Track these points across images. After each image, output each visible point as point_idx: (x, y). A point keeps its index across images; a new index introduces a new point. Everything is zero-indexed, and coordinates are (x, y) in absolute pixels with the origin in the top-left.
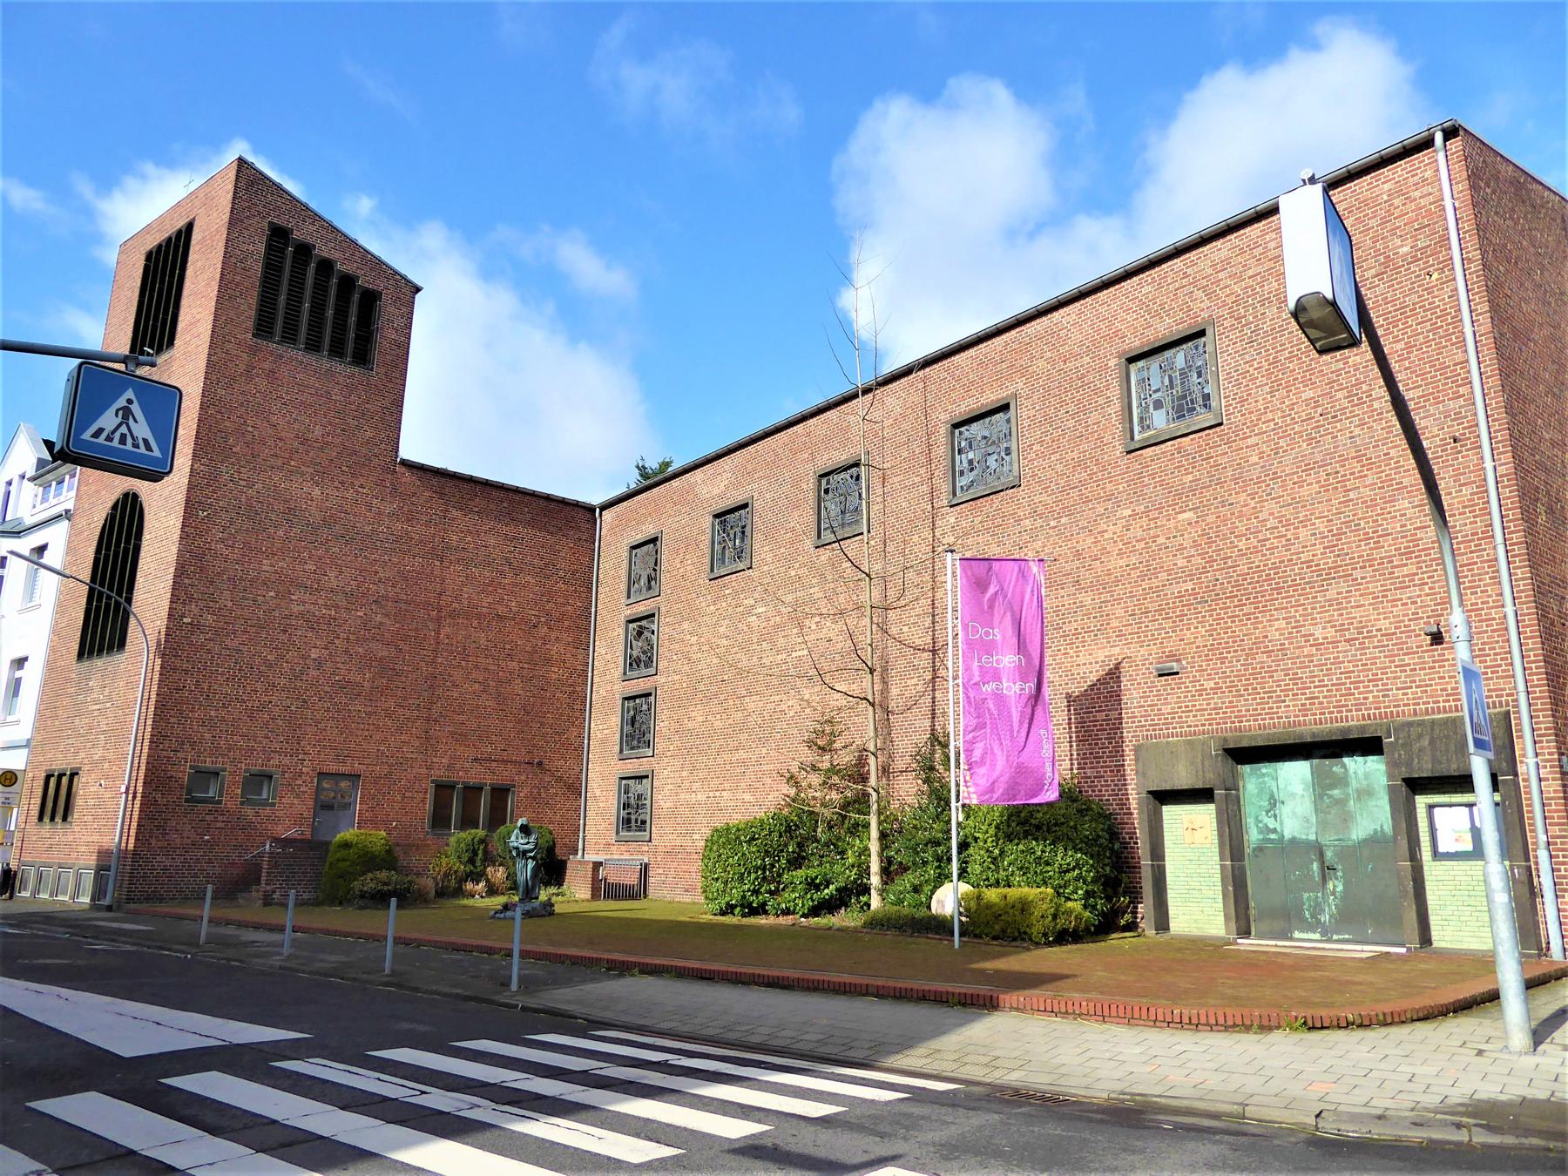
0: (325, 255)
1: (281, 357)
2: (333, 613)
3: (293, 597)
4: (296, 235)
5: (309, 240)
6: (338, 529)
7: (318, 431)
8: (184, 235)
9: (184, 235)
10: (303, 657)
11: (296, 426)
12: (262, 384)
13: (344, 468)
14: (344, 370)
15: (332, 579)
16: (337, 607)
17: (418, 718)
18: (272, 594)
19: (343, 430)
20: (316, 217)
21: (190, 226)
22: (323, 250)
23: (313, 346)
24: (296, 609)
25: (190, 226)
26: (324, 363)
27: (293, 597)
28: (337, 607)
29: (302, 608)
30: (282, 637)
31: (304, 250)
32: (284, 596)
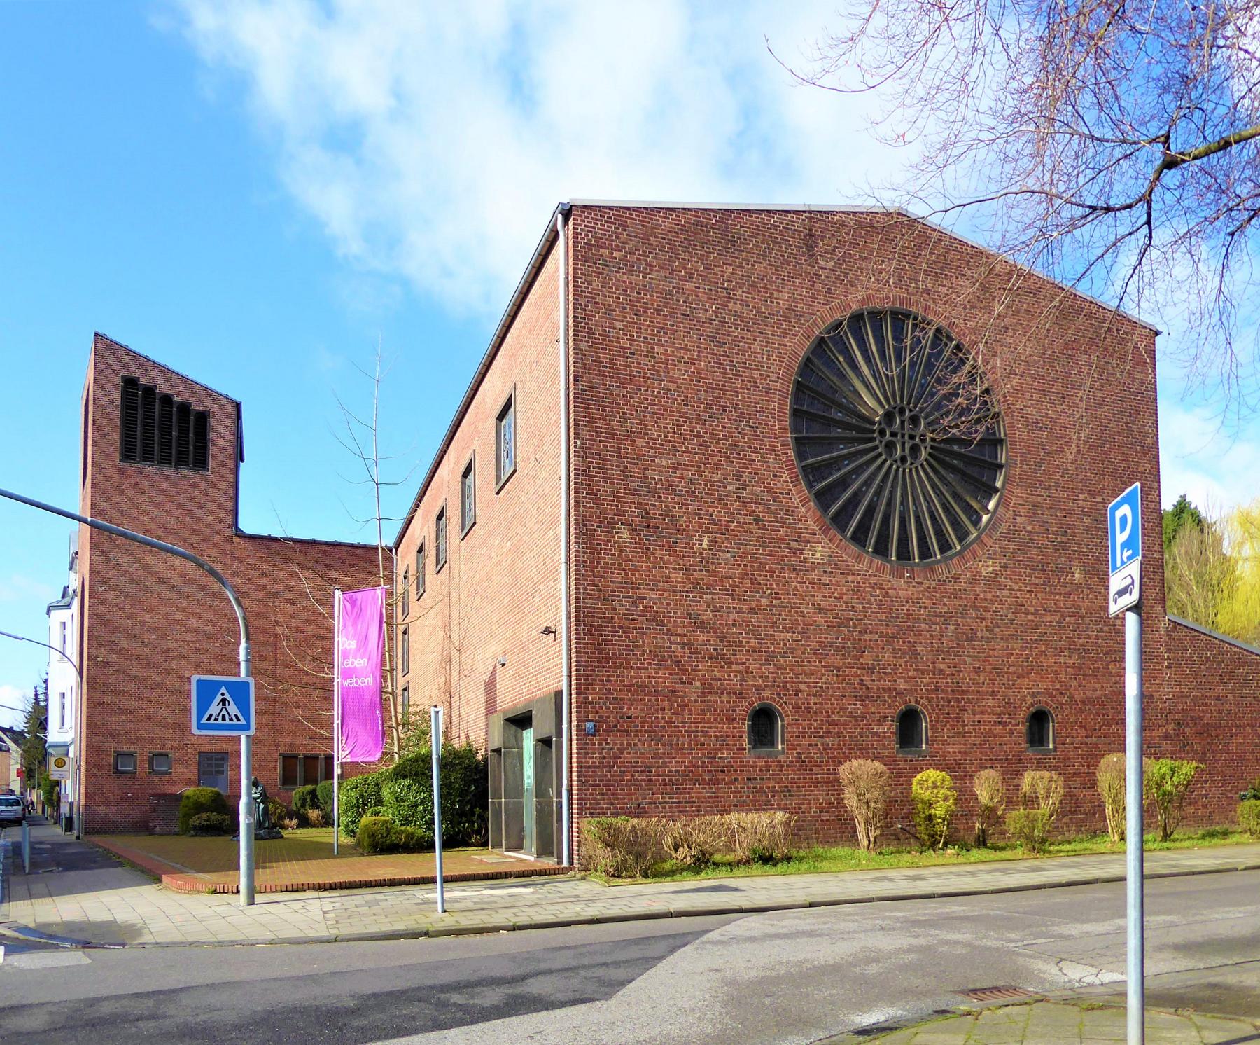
0: (164, 391)
1: (141, 473)
2: (198, 646)
3: (169, 638)
4: (142, 381)
5: (152, 383)
6: (195, 588)
7: (173, 521)
10: (181, 678)
11: (158, 520)
12: (130, 494)
13: (195, 545)
14: (186, 474)
15: (195, 623)
16: (199, 641)
17: (266, 712)
18: (153, 637)
19: (192, 518)
20: (155, 365)
22: (162, 388)
23: (165, 461)
24: (171, 645)
26: (172, 471)
27: (169, 638)
28: (199, 641)
29: (176, 645)
30: (164, 665)
31: (150, 390)
32: (163, 637)
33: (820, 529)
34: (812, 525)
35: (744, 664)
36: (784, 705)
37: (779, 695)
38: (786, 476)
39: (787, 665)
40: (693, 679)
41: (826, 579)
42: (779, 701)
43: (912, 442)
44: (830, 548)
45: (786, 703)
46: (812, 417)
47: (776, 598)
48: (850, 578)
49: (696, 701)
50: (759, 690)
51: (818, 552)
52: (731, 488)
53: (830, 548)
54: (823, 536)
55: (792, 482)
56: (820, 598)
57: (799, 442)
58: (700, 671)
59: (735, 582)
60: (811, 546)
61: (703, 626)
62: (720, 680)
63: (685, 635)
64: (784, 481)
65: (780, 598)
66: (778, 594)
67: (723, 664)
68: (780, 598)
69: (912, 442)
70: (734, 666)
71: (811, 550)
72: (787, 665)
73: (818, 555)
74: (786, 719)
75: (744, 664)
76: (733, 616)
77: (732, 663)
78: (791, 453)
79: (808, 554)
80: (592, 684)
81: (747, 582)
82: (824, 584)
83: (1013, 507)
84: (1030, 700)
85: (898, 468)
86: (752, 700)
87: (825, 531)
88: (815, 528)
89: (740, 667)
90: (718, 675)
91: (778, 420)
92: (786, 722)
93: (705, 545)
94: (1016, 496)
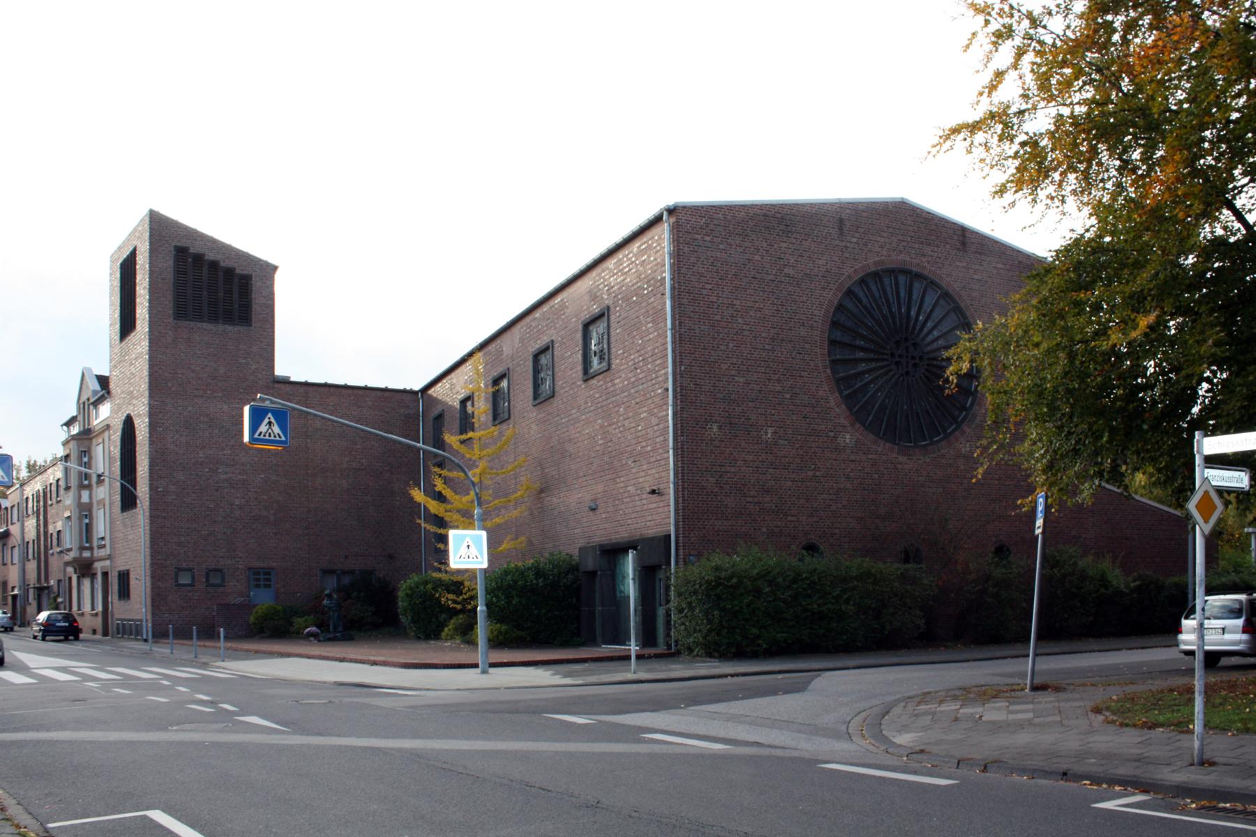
8: (133, 254)
9: (133, 254)
21: (135, 250)
25: (135, 250)
34: (842, 421)
41: (853, 458)
43: (913, 362)
46: (843, 345)
48: (870, 456)
51: (847, 438)
52: (788, 396)
56: (849, 470)
57: (834, 362)
61: (768, 491)
69: (913, 362)
70: (789, 518)
73: (848, 441)
78: (829, 371)
79: (840, 440)
80: (692, 531)
81: (798, 460)
85: (903, 380)
87: (852, 425)
89: (793, 518)
90: (779, 524)
93: (769, 436)
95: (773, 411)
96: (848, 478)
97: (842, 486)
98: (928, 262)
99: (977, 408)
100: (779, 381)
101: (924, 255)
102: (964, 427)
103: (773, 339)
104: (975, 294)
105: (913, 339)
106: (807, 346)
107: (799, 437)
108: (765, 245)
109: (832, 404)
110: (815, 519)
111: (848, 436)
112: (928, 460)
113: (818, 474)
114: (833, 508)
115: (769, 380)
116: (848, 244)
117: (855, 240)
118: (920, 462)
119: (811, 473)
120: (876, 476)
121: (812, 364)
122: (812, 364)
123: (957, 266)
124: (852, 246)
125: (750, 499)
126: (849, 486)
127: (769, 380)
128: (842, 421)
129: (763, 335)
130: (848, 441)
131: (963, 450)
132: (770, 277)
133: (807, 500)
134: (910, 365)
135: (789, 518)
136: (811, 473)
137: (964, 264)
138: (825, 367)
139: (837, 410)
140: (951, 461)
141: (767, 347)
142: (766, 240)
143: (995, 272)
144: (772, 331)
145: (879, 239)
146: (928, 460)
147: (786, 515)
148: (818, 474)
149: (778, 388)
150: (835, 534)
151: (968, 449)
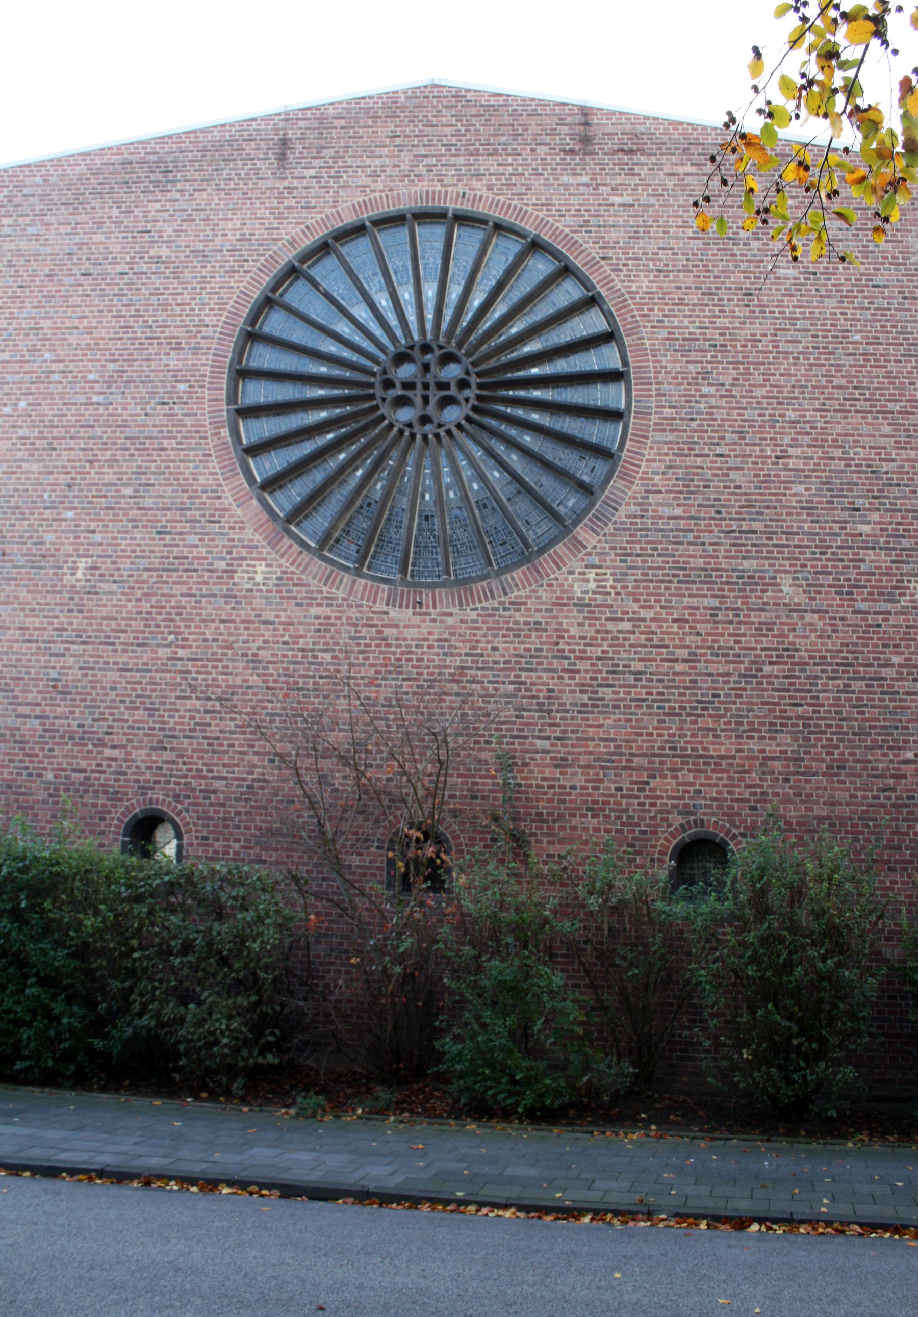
33: (265, 539)
34: (249, 534)
35: (124, 747)
36: (184, 814)
37: (176, 797)
38: (214, 465)
39: (193, 750)
40: (45, 769)
42: (176, 807)
44: (280, 566)
45: (187, 810)
47: (183, 647)
48: (313, 611)
49: (44, 802)
50: (144, 789)
52: (128, 491)
53: (280, 566)
54: (269, 549)
55: (222, 474)
58: (55, 757)
59: (120, 625)
60: (248, 565)
62: (84, 771)
63: (38, 705)
64: (211, 474)
65: (190, 647)
66: (186, 640)
67: (90, 747)
68: (190, 647)
70: (107, 752)
71: (248, 572)
72: (193, 750)
73: (259, 578)
74: (185, 836)
75: (124, 747)
76: (114, 675)
77: (105, 746)
82: (266, 622)
83: (641, 479)
84: (677, 820)
86: (132, 804)
87: (273, 543)
88: (257, 537)
89: (116, 753)
90: (83, 764)
91: (209, 389)
92: (185, 841)
93: (79, 575)
94: (647, 461)
95: (93, 525)
96: (255, 660)
97: (238, 681)
98: (490, 188)
99: (620, 484)
100: (112, 462)
101: (478, 176)
102: (581, 532)
103: (109, 383)
104: (613, 235)
105: (441, 347)
106: (182, 387)
107: (146, 575)
108: (115, 212)
109: (228, 499)
110: (167, 756)
111: (261, 567)
112: (474, 615)
113: (181, 653)
114: (214, 730)
115: (91, 462)
116: (296, 183)
117: (312, 172)
118: (450, 621)
119: (164, 652)
120: (328, 656)
121: (188, 421)
122: (188, 421)
123: (566, 186)
124: (305, 183)
125: (25, 710)
126: (254, 680)
127: (91, 462)
128: (249, 534)
129: (91, 377)
130: (259, 578)
131: (578, 591)
132: (119, 269)
133: (152, 712)
134: (433, 401)
135: (107, 752)
136: (164, 652)
137: (585, 179)
138: (217, 425)
139: (239, 512)
140: (538, 617)
141: (95, 399)
142: (118, 204)
143: (670, 183)
144: (111, 366)
145: (368, 161)
146: (474, 615)
147: (100, 744)
148: (181, 653)
149: (112, 478)
150: (214, 792)
151: (592, 585)
